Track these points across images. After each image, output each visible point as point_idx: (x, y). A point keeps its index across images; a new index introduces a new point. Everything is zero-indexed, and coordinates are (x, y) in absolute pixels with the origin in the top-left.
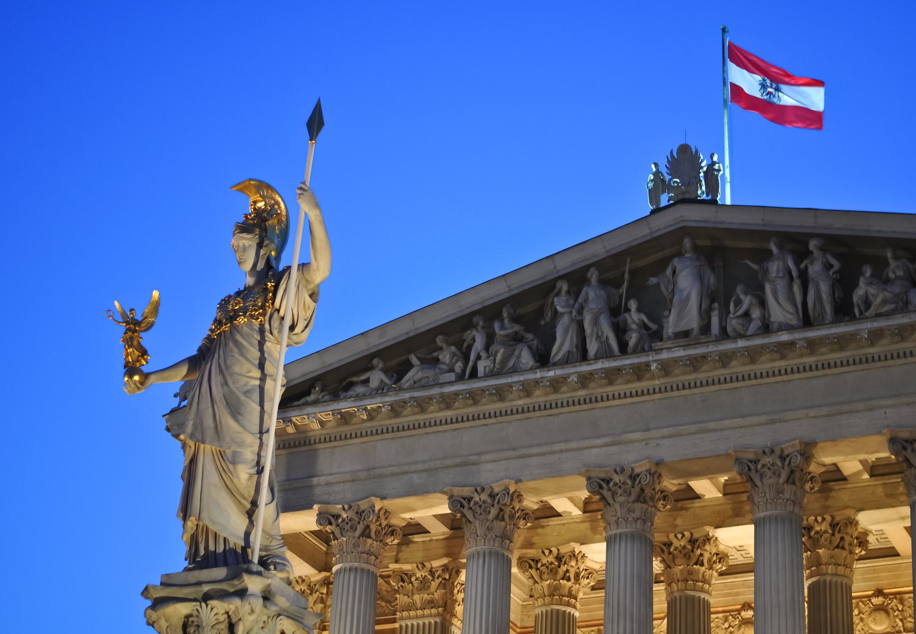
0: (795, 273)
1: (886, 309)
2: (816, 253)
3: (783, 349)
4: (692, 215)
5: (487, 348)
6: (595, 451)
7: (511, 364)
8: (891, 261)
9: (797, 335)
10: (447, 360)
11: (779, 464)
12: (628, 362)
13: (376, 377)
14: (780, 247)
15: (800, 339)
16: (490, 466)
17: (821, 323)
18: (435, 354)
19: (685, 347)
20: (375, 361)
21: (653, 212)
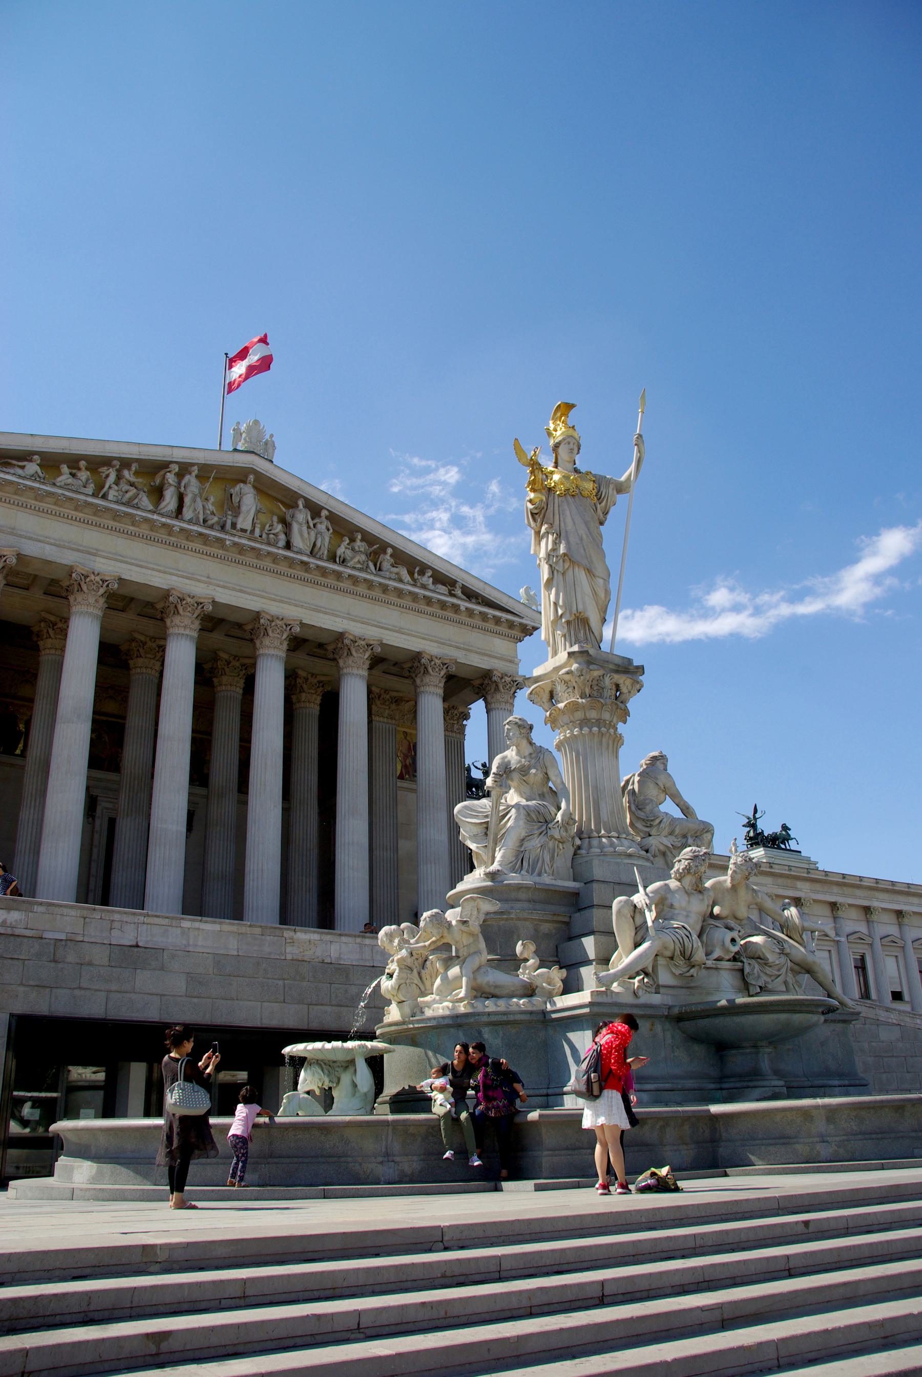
0: (312, 525)
1: (359, 566)
2: (323, 519)
3: (291, 562)
4: (261, 465)
5: (117, 483)
6: (175, 578)
7: (136, 501)
8: (358, 541)
9: (311, 560)
10: (84, 478)
11: (284, 627)
12: (213, 533)
13: (32, 468)
14: (305, 507)
15: (313, 563)
16: (102, 560)
17: (321, 559)
18: (74, 471)
19: (249, 539)
20: (36, 457)
21: (235, 450)
